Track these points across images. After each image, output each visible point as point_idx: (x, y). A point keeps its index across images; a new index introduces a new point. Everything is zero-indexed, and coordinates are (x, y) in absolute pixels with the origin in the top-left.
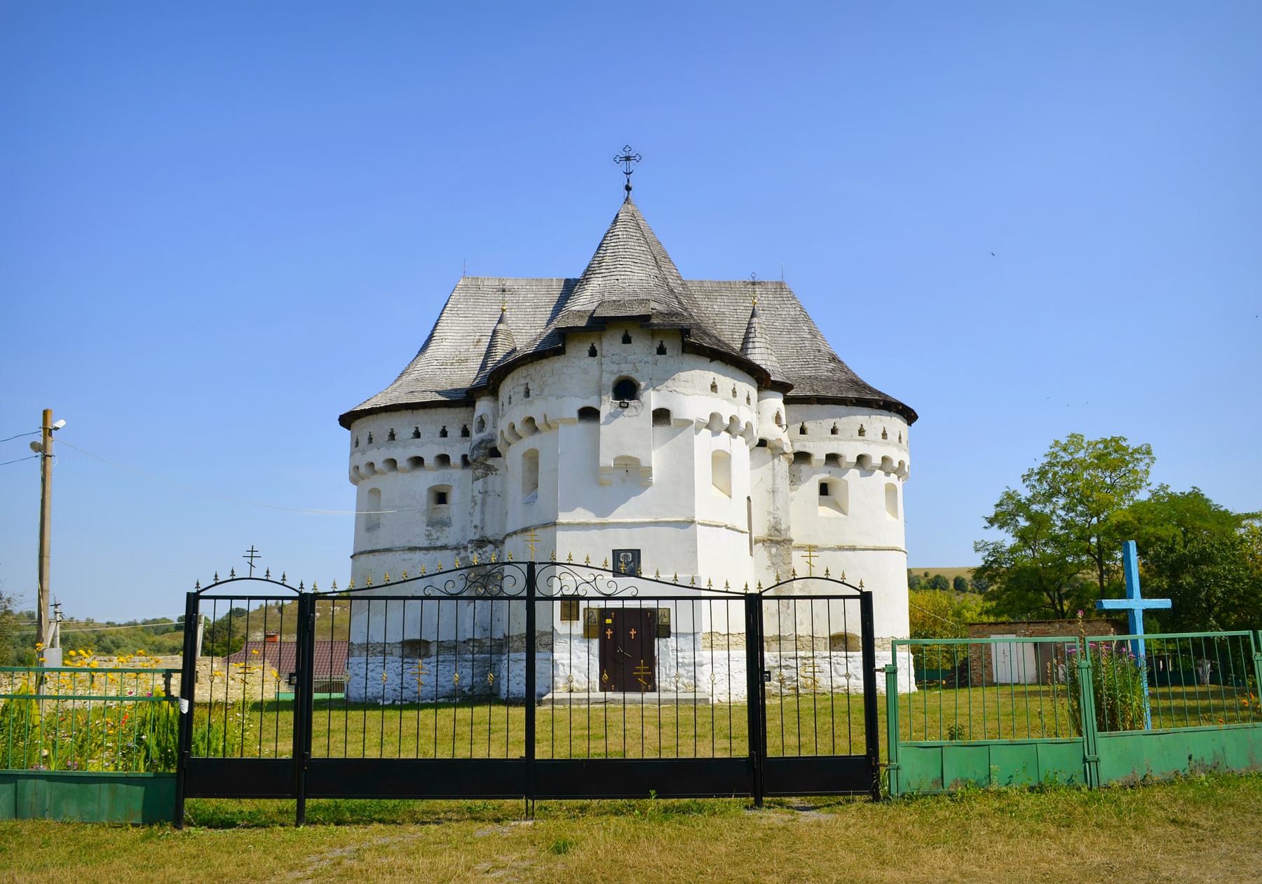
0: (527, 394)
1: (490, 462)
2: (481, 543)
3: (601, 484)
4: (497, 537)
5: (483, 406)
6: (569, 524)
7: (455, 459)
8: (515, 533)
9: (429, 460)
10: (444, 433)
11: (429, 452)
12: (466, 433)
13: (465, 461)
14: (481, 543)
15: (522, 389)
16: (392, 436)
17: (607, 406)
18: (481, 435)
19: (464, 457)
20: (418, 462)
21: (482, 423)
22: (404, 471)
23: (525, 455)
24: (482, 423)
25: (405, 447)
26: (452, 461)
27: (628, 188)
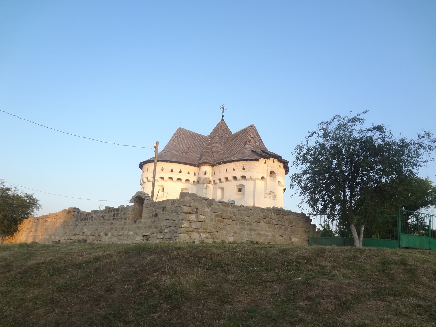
0: (244, 169)
1: (208, 185)
9: (184, 180)
10: (189, 173)
11: (184, 177)
12: (195, 174)
15: (242, 168)
16: (172, 171)
17: (268, 178)
18: (205, 176)
19: (194, 181)
20: (179, 179)
21: (205, 174)
22: (175, 182)
23: (237, 186)
27: (223, 116)
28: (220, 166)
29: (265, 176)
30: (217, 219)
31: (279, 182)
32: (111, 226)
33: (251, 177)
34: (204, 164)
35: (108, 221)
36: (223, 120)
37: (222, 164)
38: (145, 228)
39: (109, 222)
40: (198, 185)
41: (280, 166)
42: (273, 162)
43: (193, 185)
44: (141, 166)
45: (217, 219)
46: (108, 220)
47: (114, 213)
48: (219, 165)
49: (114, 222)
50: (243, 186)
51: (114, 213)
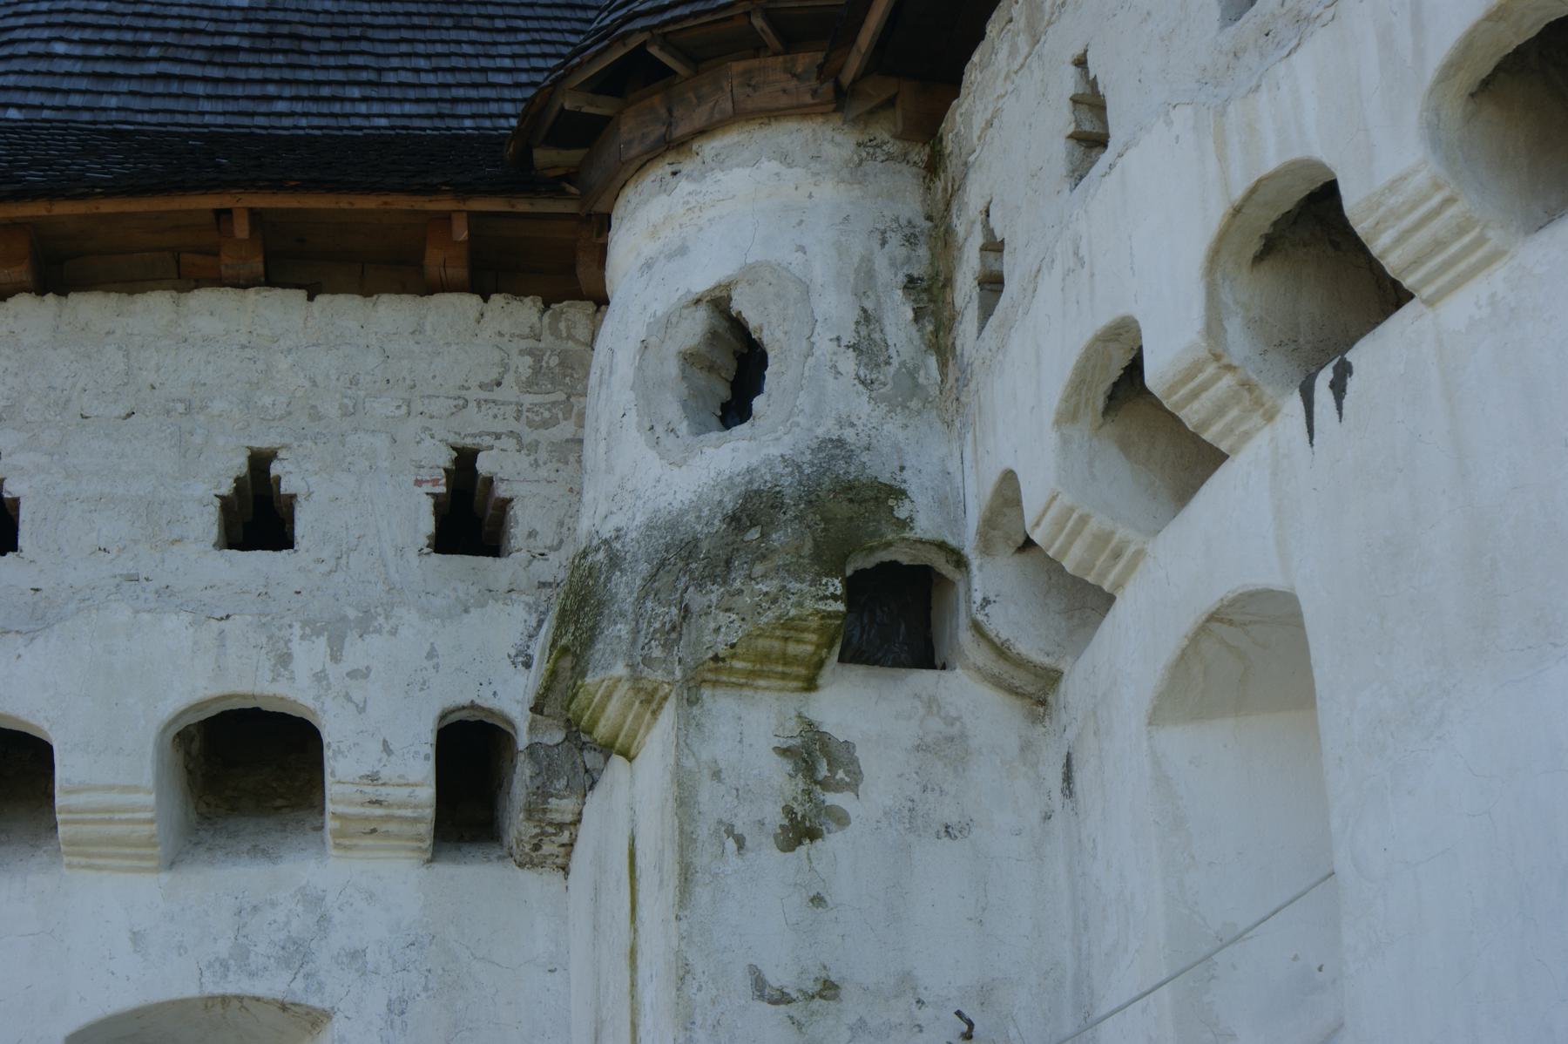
5: (730, 213)
7: (379, 754)
10: (258, 516)
12: (468, 518)
13: (474, 782)
26: (343, 770)
43: (475, 878)
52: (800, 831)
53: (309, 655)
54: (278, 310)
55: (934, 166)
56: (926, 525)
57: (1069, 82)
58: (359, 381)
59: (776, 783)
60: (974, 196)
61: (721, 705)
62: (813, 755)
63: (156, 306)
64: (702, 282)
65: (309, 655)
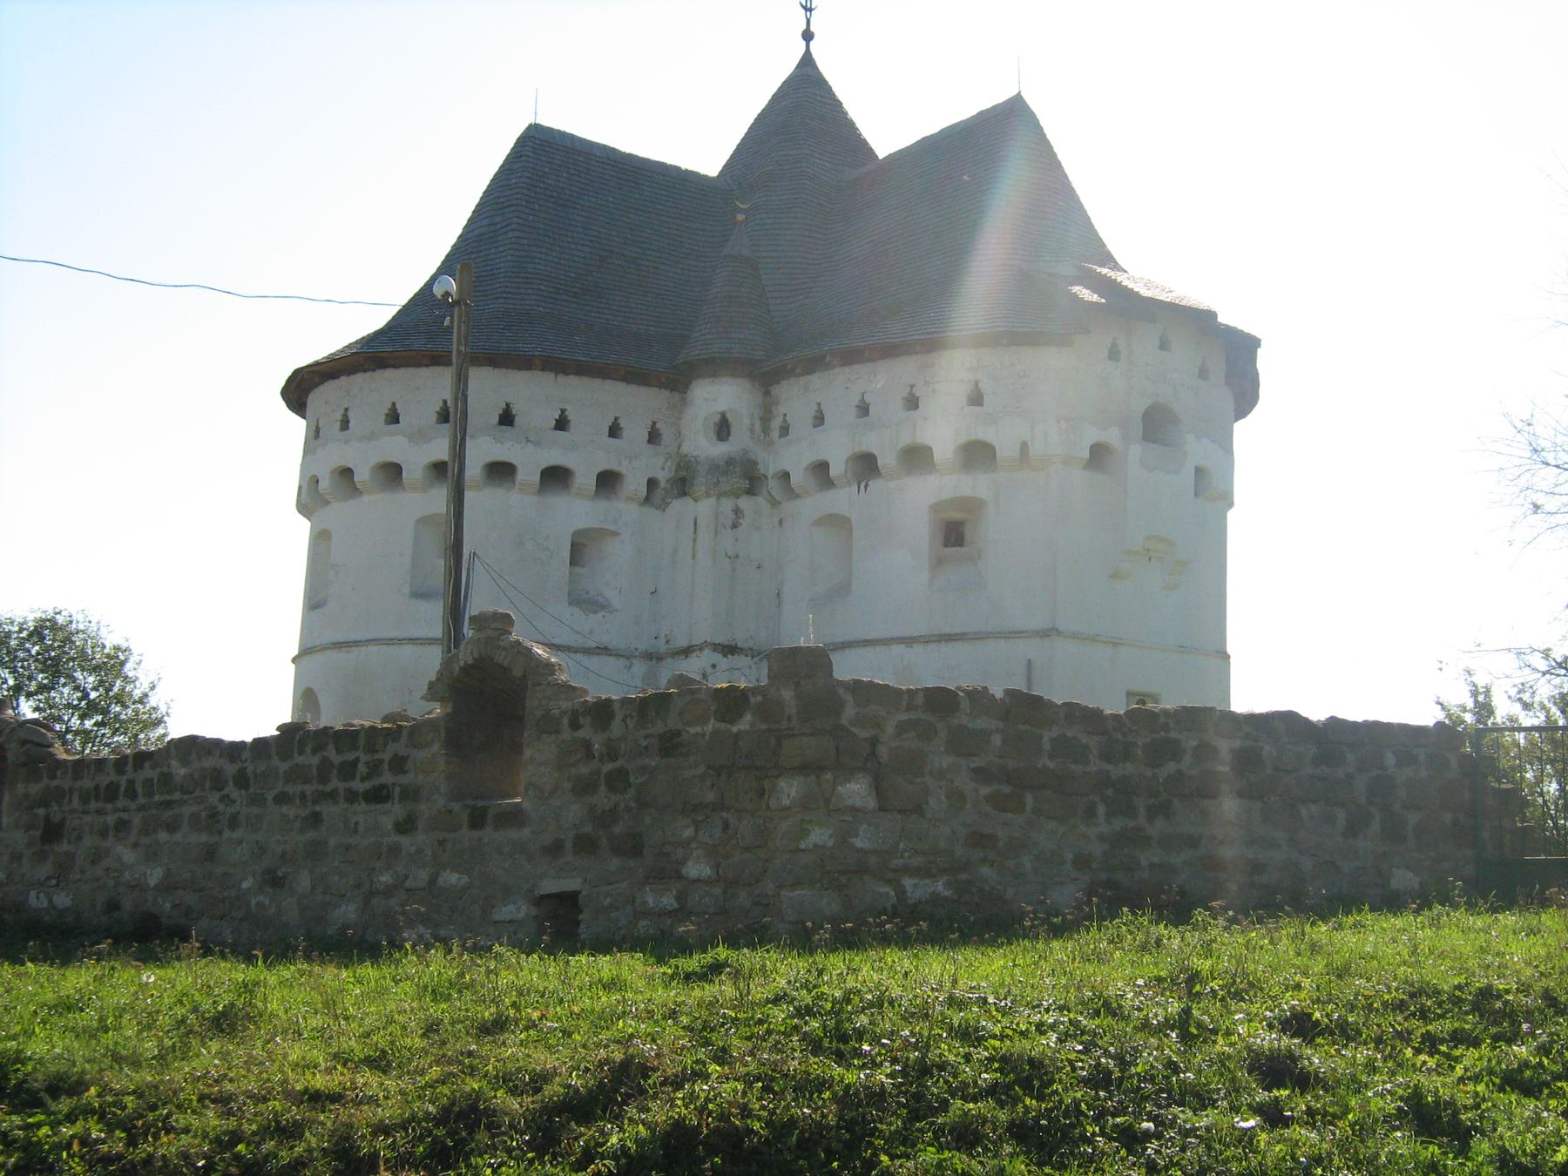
1: (745, 503)
2: (729, 650)
3: (1114, 576)
4: (750, 644)
6: (1074, 636)
7: (635, 483)
8: (908, 641)
9: (585, 478)
10: (614, 431)
12: (654, 437)
14: (729, 650)
19: (652, 483)
20: (556, 477)
21: (723, 429)
23: (936, 508)
24: (723, 429)
25: (537, 444)
27: (808, 36)
28: (816, 379)
29: (1112, 437)
30: (985, 790)
31: (1199, 471)
32: (311, 835)
33: (1024, 446)
34: (713, 366)
35: (285, 809)
36: (807, 61)
37: (829, 367)
38: (555, 849)
39: (290, 811)
40: (677, 505)
41: (1203, 373)
42: (1164, 345)
44: (300, 390)
45: (985, 790)
46: (282, 799)
47: (324, 760)
48: (810, 372)
49: (329, 810)
50: (973, 506)
51: (324, 760)
52: (734, 526)
53: (625, 463)
54: (621, 387)
55: (767, 393)
56: (762, 471)
57: (815, 407)
58: (638, 405)
59: (731, 515)
60: (782, 409)
61: (724, 500)
62: (737, 511)
63: (597, 382)
64: (721, 409)
65: (625, 463)
